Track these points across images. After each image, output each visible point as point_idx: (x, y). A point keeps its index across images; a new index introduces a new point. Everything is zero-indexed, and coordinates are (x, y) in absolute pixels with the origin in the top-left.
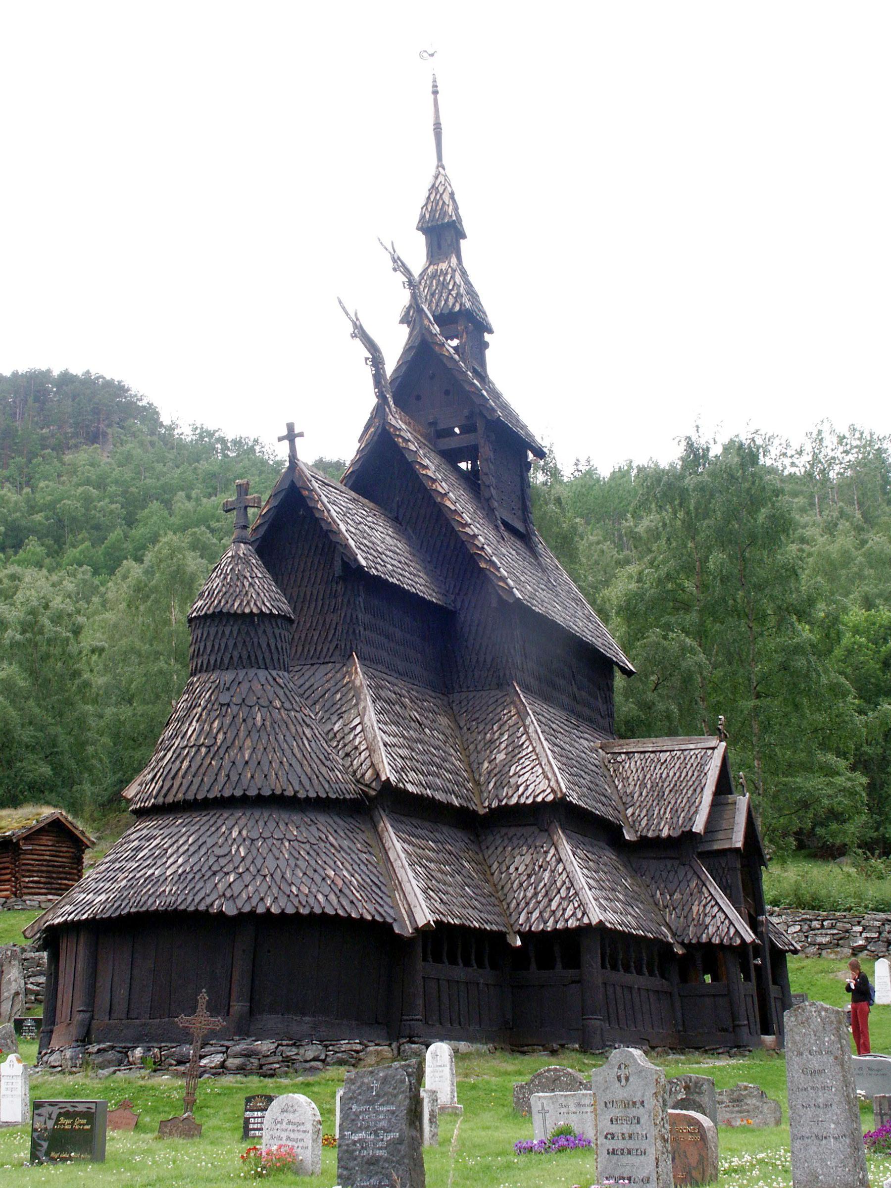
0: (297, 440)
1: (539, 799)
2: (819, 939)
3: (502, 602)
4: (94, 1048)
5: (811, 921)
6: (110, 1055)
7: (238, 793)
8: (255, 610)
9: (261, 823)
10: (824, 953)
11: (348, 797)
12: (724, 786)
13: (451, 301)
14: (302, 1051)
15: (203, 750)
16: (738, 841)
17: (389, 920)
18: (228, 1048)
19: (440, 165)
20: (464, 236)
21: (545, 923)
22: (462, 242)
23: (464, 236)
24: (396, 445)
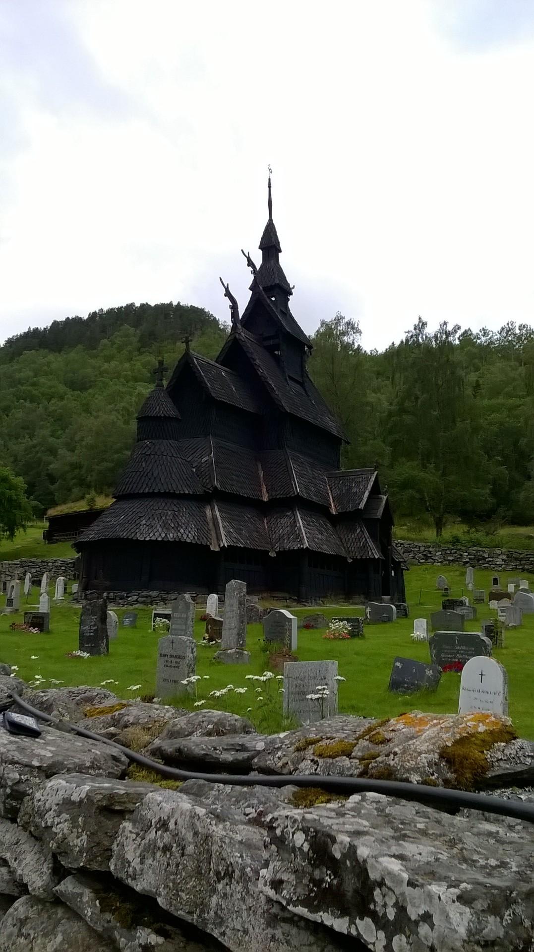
0: (190, 343)
2: (449, 558)
4: (88, 592)
5: (446, 550)
6: (95, 595)
7: (151, 491)
8: (162, 415)
9: (159, 504)
10: (451, 564)
11: (198, 493)
12: (376, 490)
14: (169, 596)
16: (380, 513)
17: (208, 543)
18: (139, 594)
19: (271, 220)
20: (280, 251)
22: (280, 254)
23: (280, 251)
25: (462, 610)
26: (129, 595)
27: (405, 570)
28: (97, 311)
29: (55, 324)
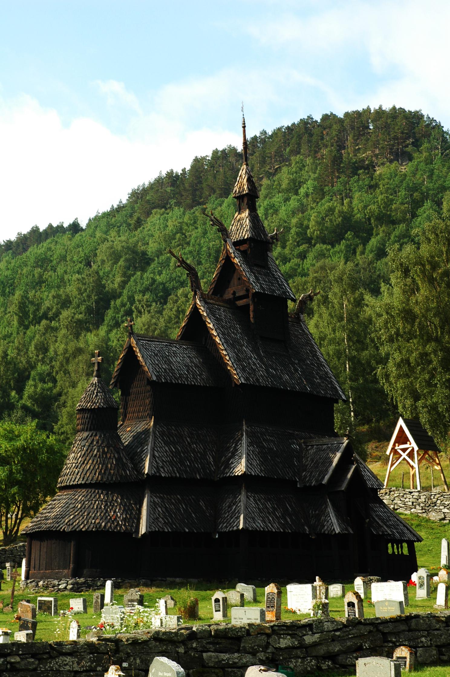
1: (236, 474)
3: (236, 384)
4: (29, 581)
6: (33, 584)
13: (244, 233)
15: (74, 465)
16: (343, 487)
21: (227, 528)
24: (199, 312)
25: (333, 588)
26: (60, 583)
27: (415, 541)
28: (258, 135)
29: (198, 163)
